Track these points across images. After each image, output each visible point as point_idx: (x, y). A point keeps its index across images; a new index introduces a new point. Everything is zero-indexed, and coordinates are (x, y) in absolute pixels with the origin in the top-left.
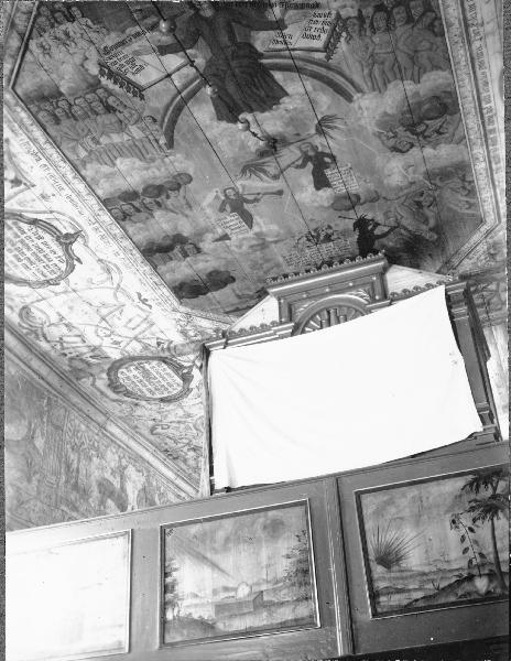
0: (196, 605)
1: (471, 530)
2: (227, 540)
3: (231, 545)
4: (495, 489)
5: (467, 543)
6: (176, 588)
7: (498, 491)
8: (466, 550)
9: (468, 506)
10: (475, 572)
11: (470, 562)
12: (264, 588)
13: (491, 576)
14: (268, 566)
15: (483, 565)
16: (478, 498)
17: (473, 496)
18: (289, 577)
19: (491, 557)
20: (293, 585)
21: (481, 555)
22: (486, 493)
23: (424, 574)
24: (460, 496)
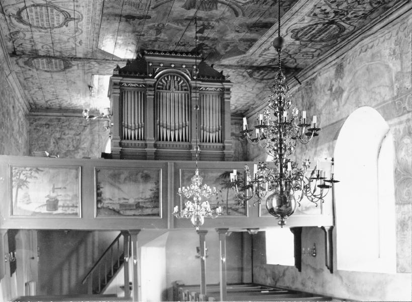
0: (111, 203)
1: (220, 191)
2: (125, 179)
3: (127, 182)
5: (218, 196)
6: (102, 195)
8: (217, 198)
9: (221, 182)
11: (218, 203)
12: (140, 201)
13: (224, 208)
14: (142, 193)
15: (223, 204)
16: (225, 180)
18: (151, 198)
19: (225, 202)
20: (152, 201)
21: (223, 201)
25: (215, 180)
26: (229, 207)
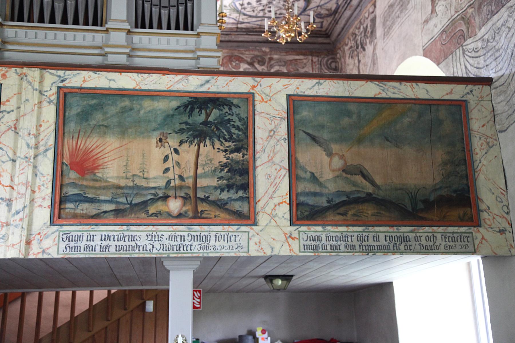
1: (176, 151)
4: (208, 115)
5: (169, 164)
7: (210, 119)
8: (167, 170)
9: (178, 127)
10: (171, 193)
11: (169, 182)
13: (186, 199)
15: (181, 188)
16: (190, 121)
17: (185, 118)
19: (190, 182)
21: (181, 178)
22: (199, 118)
23: (119, 187)
24: (173, 115)
25: (160, 119)
26: (201, 194)
